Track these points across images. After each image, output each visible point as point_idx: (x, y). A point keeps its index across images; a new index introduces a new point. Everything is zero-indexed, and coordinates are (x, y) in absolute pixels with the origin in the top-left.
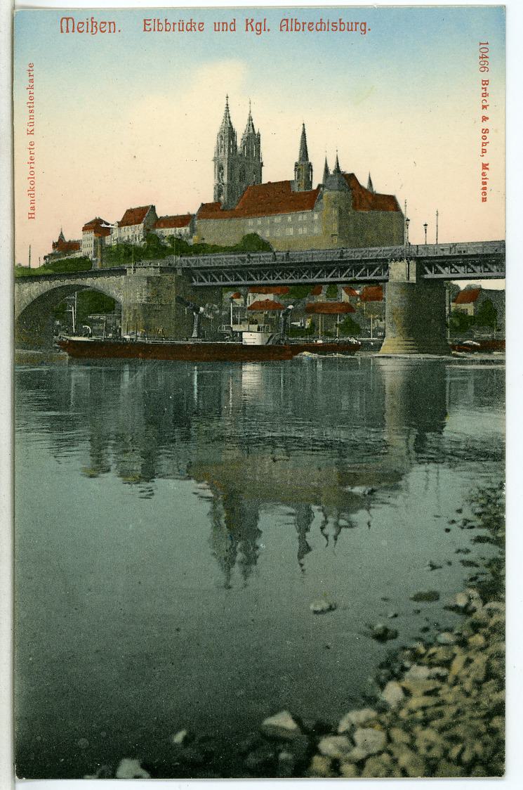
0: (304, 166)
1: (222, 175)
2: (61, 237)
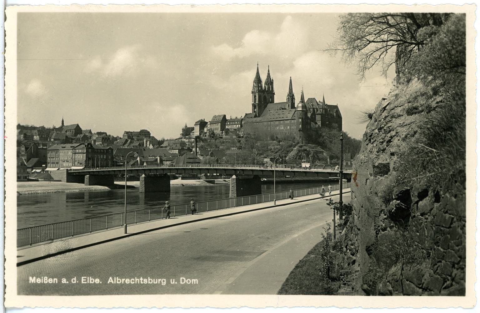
0: (291, 96)
1: (256, 99)
2: (186, 126)
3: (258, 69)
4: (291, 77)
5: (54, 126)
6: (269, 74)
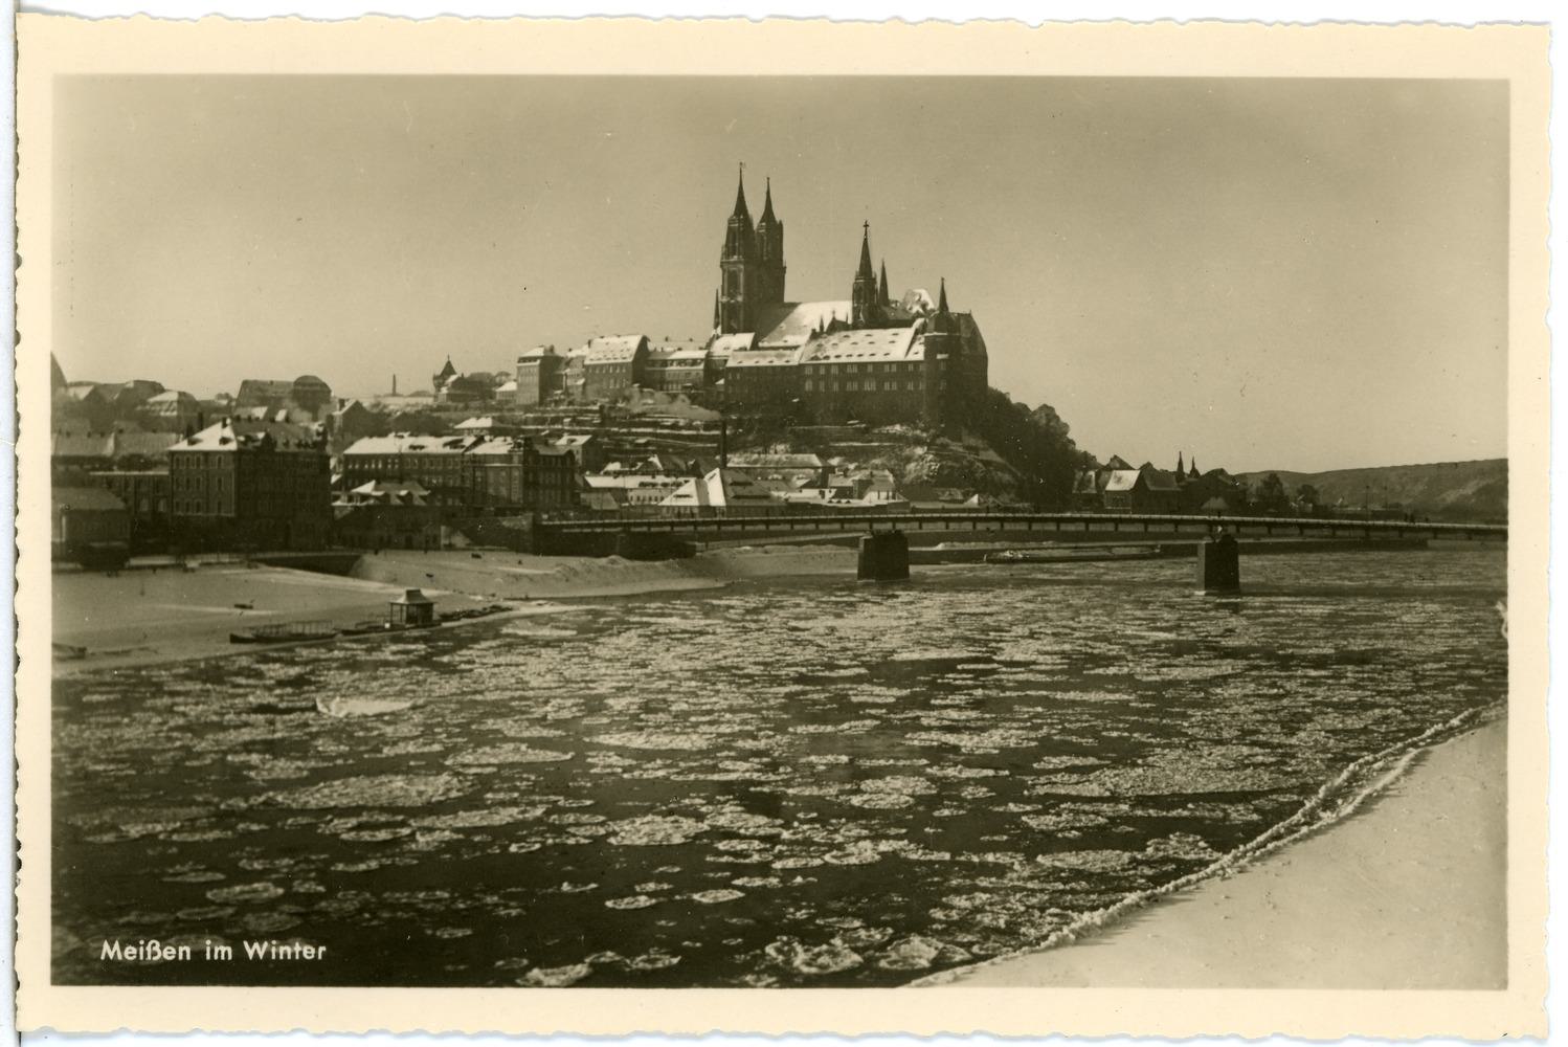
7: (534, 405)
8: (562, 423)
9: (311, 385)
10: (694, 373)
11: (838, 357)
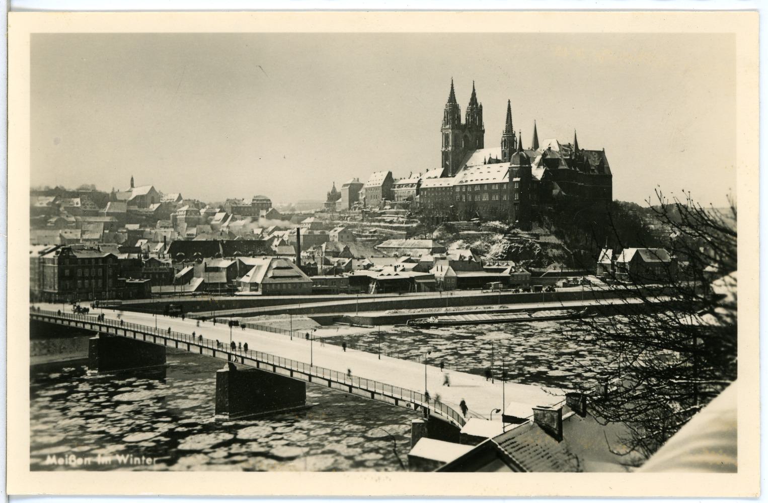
1: (448, 143)
3: (452, 88)
4: (509, 102)
5: (113, 189)
6: (474, 94)
7: (346, 210)
8: (347, 220)
9: (261, 200)
10: (412, 191)
11: (472, 181)
